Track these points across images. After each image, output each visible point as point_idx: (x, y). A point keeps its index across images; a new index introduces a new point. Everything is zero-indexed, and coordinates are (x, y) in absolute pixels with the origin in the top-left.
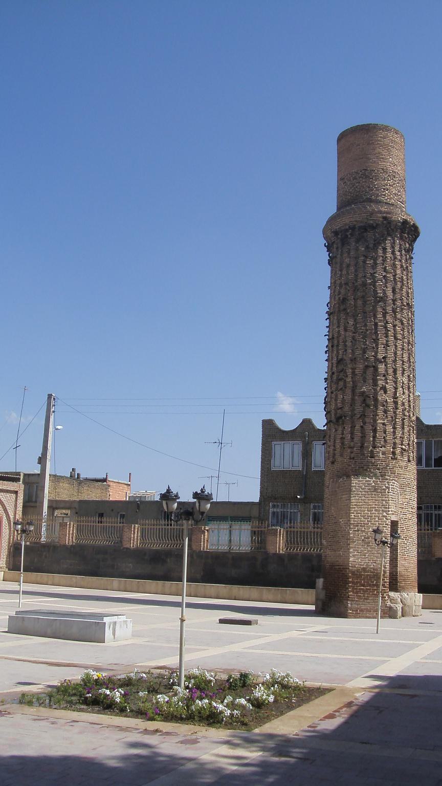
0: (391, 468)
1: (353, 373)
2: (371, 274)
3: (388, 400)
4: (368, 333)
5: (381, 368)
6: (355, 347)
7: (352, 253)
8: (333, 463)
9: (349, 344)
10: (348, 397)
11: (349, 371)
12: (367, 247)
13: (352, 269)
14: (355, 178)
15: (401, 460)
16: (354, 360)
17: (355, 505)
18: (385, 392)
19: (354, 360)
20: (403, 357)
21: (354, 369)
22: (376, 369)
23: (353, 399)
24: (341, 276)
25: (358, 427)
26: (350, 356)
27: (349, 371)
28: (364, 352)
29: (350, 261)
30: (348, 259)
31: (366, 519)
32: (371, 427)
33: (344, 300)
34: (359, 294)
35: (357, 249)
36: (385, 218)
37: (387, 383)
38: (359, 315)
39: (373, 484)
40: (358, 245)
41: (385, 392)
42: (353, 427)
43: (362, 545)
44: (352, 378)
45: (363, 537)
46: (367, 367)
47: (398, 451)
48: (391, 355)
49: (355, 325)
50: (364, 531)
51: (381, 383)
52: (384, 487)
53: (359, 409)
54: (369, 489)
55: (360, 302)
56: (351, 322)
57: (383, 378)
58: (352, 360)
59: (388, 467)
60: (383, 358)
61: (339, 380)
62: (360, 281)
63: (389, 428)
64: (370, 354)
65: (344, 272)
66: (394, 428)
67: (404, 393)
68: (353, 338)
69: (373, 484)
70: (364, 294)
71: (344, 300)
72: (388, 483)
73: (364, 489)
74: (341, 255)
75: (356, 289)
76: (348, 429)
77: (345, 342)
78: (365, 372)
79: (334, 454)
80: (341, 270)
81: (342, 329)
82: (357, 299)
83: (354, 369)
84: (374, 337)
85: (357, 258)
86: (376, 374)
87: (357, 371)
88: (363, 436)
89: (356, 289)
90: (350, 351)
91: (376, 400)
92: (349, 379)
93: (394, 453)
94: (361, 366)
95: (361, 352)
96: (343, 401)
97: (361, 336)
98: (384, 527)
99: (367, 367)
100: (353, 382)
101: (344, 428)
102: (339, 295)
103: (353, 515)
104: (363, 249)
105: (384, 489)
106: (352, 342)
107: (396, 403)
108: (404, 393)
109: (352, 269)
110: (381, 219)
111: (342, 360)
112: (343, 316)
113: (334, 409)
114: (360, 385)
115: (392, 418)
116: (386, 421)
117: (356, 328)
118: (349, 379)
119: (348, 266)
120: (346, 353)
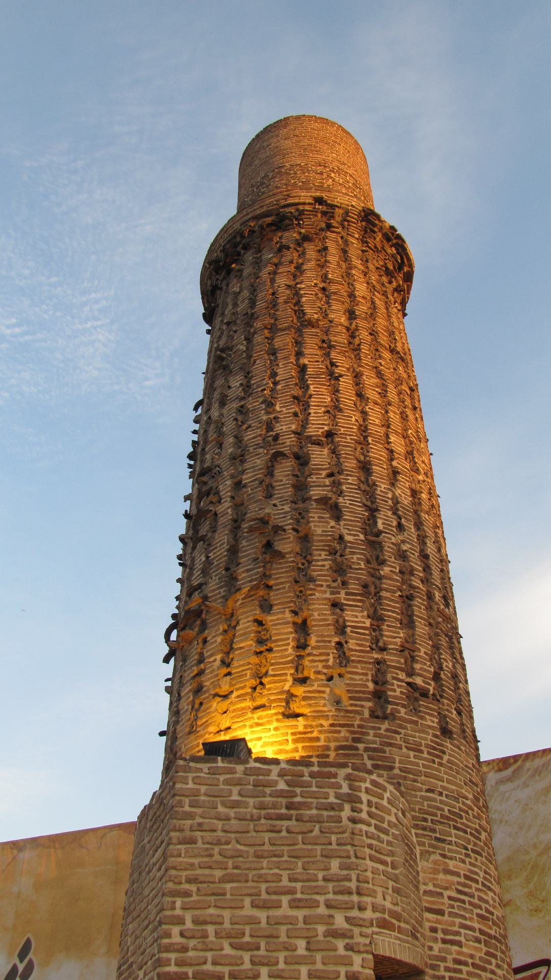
0: (374, 750)
3: (348, 538)
5: (320, 456)
15: (416, 723)
17: (189, 881)
18: (338, 517)
20: (389, 443)
32: (288, 616)
36: (319, 201)
37: (341, 493)
39: (282, 786)
41: (338, 517)
44: (233, 498)
46: (278, 456)
47: (396, 690)
48: (349, 422)
52: (332, 799)
54: (262, 807)
59: (361, 746)
60: (330, 435)
63: (357, 617)
66: (377, 619)
67: (400, 527)
69: (282, 786)
73: (236, 805)
78: (270, 474)
84: (297, 392)
90: (231, 440)
91: (305, 539)
93: (379, 695)
97: (261, 400)
101: (205, 641)
103: (176, 930)
105: (331, 807)
106: (236, 420)
108: (400, 527)
116: (342, 595)
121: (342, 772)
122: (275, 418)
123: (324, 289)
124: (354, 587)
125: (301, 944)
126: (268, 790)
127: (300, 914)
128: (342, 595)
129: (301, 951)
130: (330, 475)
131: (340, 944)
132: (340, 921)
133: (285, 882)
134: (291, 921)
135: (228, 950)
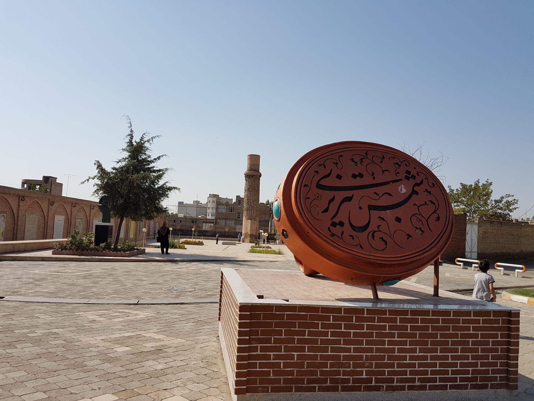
7: (251, 180)
12: (254, 179)
16: (250, 200)
22: (254, 201)
25: (251, 211)
34: (252, 188)
42: (250, 211)
51: (255, 204)
53: (251, 208)
55: (252, 190)
62: (252, 186)
63: (256, 212)
64: (253, 199)
76: (249, 211)
81: (248, 194)
85: (251, 181)
88: (251, 213)
89: (251, 187)
92: (249, 203)
94: (251, 201)
118: (249, 203)
119: (250, 182)
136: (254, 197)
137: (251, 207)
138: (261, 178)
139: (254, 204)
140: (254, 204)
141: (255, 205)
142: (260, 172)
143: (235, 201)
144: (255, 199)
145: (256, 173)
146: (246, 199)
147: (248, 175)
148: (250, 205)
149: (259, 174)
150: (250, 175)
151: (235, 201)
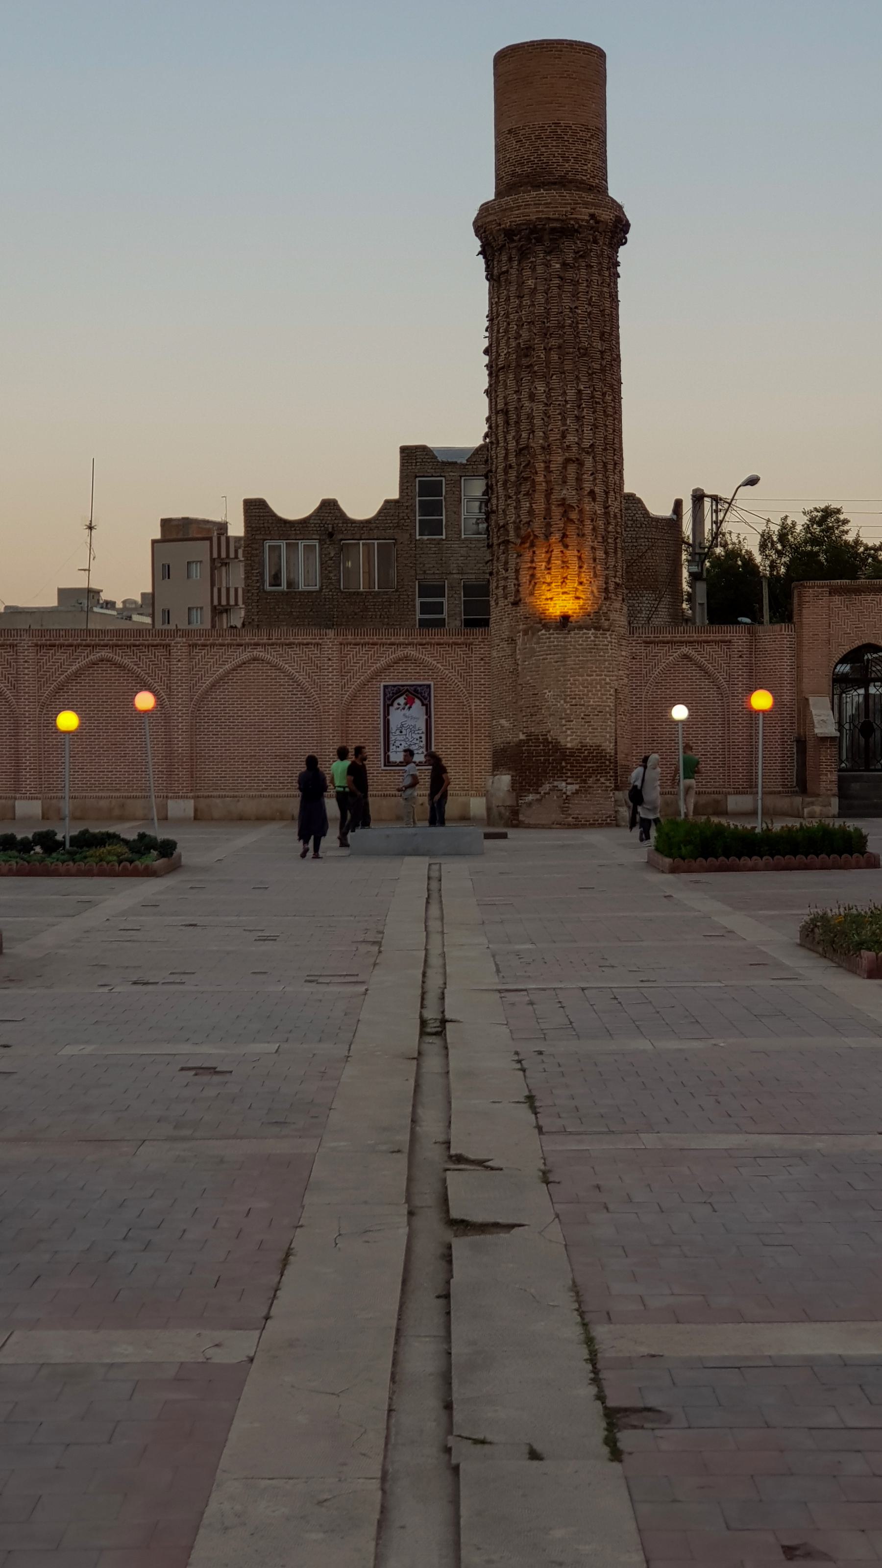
1: (547, 468)
2: (571, 309)
4: (568, 406)
5: (589, 462)
6: (549, 428)
7: (540, 269)
8: (516, 603)
9: (538, 422)
10: (540, 506)
11: (540, 466)
12: (564, 264)
13: (540, 298)
14: (539, 138)
15: (616, 600)
16: (547, 449)
18: (594, 500)
19: (547, 449)
20: (614, 444)
21: (548, 463)
22: (581, 464)
23: (548, 510)
24: (520, 306)
26: (541, 441)
27: (540, 466)
28: (564, 436)
29: (536, 284)
30: (533, 281)
31: (585, 687)
32: (576, 553)
33: (527, 351)
34: (553, 342)
35: (547, 265)
38: (554, 377)
39: (592, 638)
40: (548, 258)
41: (594, 500)
42: (549, 551)
43: (582, 725)
45: (582, 715)
49: (548, 393)
50: (583, 705)
51: (587, 486)
55: (554, 356)
56: (541, 388)
57: (591, 478)
58: (543, 448)
60: (592, 446)
61: (521, 480)
63: (600, 554)
64: (571, 438)
65: (526, 301)
68: (545, 413)
69: (592, 638)
70: (561, 341)
71: (527, 351)
72: (611, 635)
74: (520, 271)
75: (546, 334)
77: (530, 417)
78: (565, 468)
79: (518, 591)
80: (520, 297)
82: (550, 349)
83: (548, 463)
86: (581, 471)
87: (553, 466)
89: (546, 334)
90: (541, 434)
91: (581, 511)
92: (540, 478)
95: (558, 437)
96: (531, 512)
97: (558, 411)
98: (607, 698)
99: (568, 461)
100: (546, 482)
101: (534, 552)
102: (516, 338)
103: (569, 683)
104: (558, 266)
106: (543, 419)
107: (606, 514)
109: (540, 298)
110: (587, 218)
111: (527, 447)
112: (526, 376)
113: (514, 522)
114: (558, 488)
115: (603, 537)
116: (596, 543)
117: (549, 397)
118: (540, 478)
119: (534, 291)
120: (534, 436)
121: (608, 633)
122: (567, 430)
123: (590, 313)
124: (600, 539)
125: (598, 686)
126: (589, 640)
127: (598, 678)
128: (596, 543)
129: (599, 688)
130: (592, 474)
131: (608, 686)
132: (608, 680)
133: (594, 669)
134: (596, 680)
135: (581, 688)
136: (578, 418)
137: (556, 512)
138: (623, 253)
139: (579, 488)
140: (579, 488)
141: (592, 493)
142: (612, 193)
143: (395, 495)
144: (586, 444)
145: (586, 204)
146: (512, 445)
147: (510, 234)
148: (548, 493)
149: (606, 216)
150: (534, 230)
151: (395, 495)
